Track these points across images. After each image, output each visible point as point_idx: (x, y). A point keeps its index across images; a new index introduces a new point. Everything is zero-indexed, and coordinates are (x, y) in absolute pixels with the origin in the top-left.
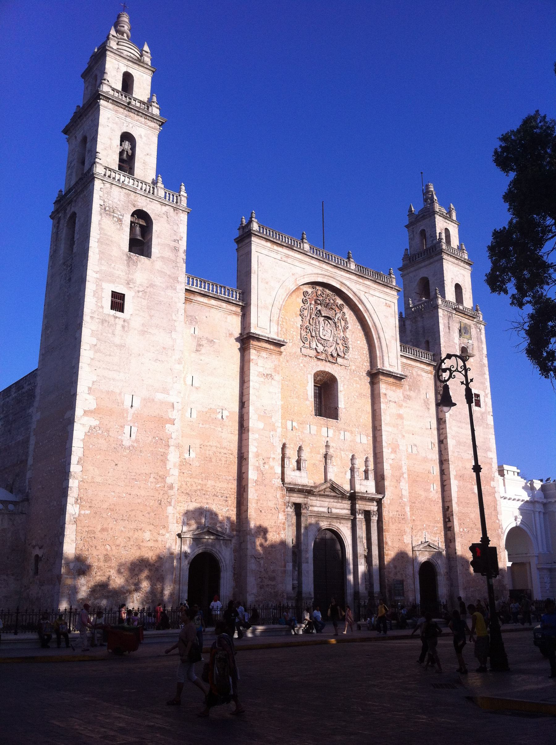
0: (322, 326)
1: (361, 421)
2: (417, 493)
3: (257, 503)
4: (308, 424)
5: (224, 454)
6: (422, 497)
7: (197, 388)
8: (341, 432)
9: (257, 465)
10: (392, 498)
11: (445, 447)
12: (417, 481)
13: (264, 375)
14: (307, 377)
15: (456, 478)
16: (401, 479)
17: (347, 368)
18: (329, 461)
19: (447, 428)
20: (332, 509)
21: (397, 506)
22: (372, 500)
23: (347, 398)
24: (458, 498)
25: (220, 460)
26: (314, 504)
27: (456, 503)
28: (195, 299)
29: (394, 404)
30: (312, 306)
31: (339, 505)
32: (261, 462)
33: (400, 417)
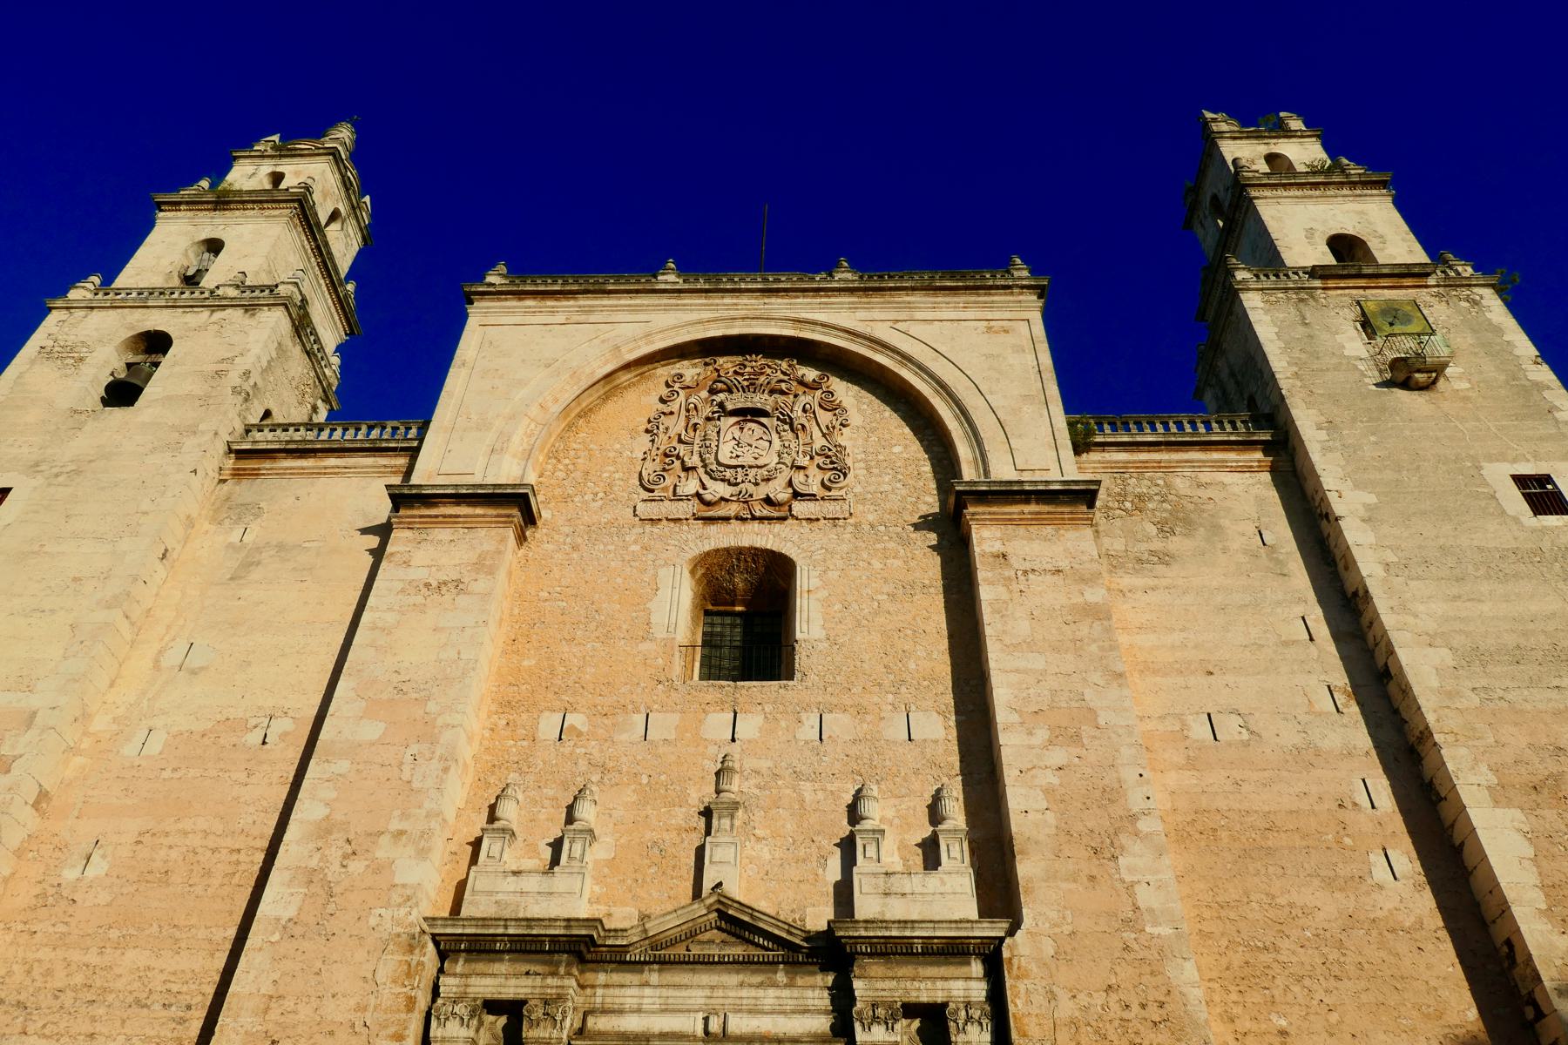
0: (729, 436)
1: (912, 666)
2: (1282, 901)
3: (266, 1010)
4: (638, 712)
5: (232, 851)
6: (1320, 916)
7: (194, 672)
8: (804, 716)
9: (314, 863)
10: (1067, 929)
11: (1399, 685)
12: (1269, 851)
13: (428, 585)
14: (656, 575)
15: (1497, 803)
16: (1124, 839)
17: (841, 522)
18: (726, 822)
19: (1381, 611)
20: (731, 1016)
21: (1107, 963)
22: (951, 951)
23: (838, 607)
24: (1549, 888)
25: (207, 873)
26: (630, 1002)
27: (1548, 913)
28: (268, 466)
29: (1049, 577)
30: (692, 400)
31: (769, 997)
32: (335, 854)
33: (1097, 613)
